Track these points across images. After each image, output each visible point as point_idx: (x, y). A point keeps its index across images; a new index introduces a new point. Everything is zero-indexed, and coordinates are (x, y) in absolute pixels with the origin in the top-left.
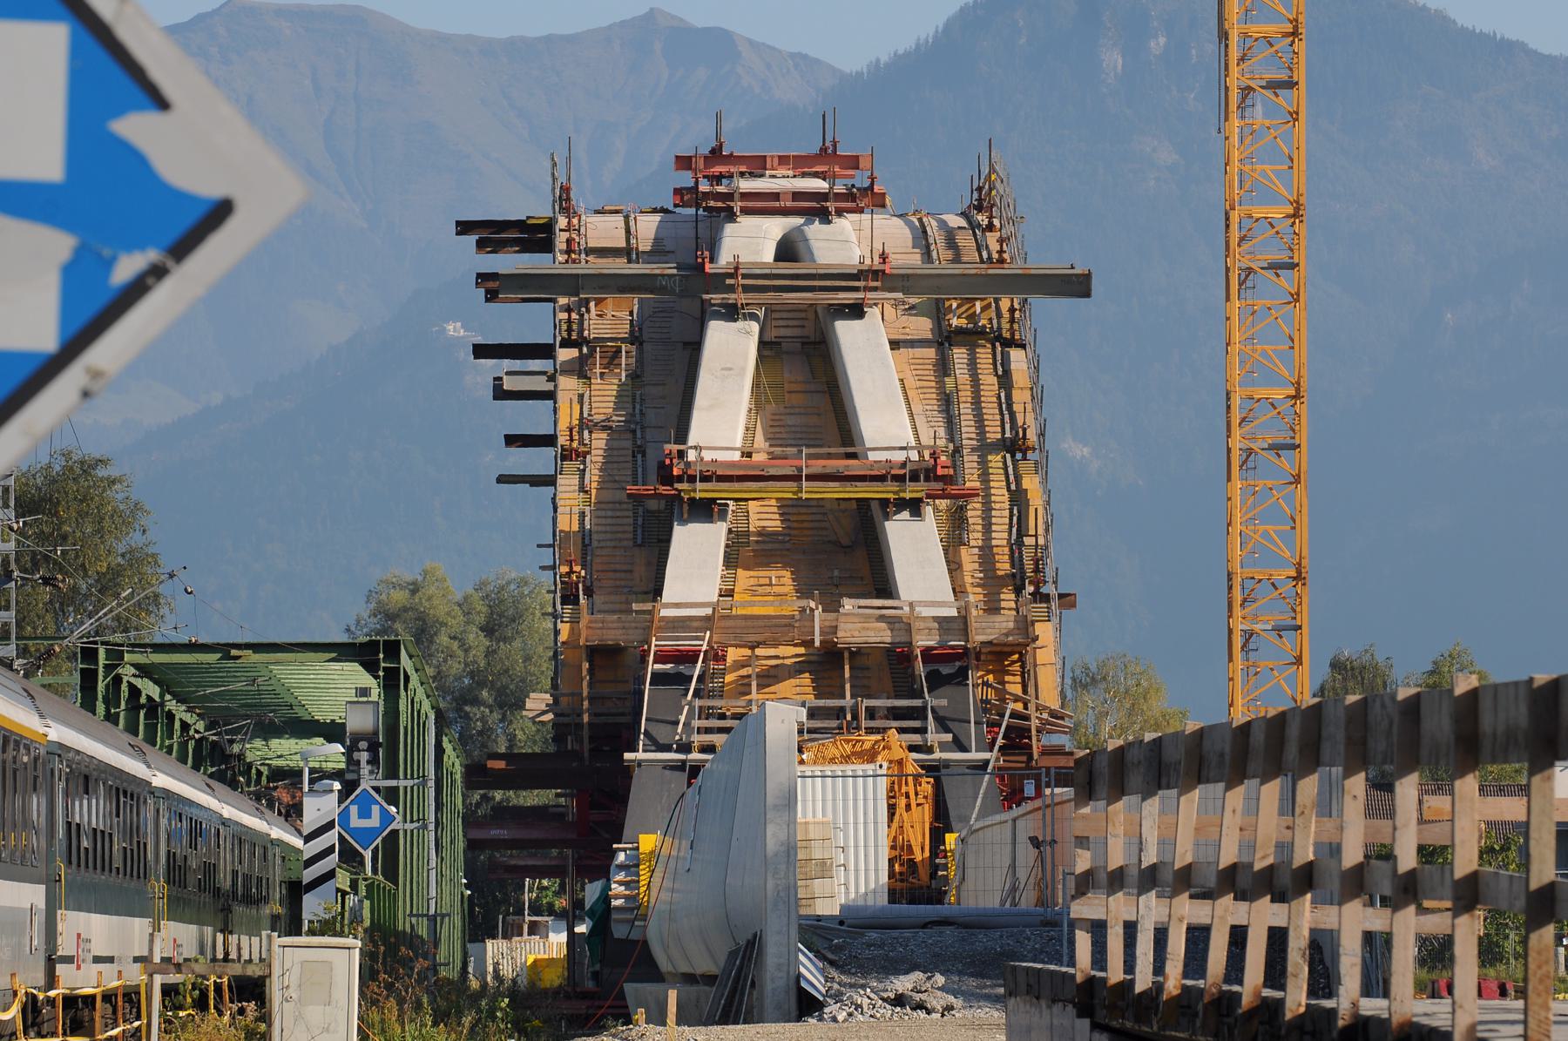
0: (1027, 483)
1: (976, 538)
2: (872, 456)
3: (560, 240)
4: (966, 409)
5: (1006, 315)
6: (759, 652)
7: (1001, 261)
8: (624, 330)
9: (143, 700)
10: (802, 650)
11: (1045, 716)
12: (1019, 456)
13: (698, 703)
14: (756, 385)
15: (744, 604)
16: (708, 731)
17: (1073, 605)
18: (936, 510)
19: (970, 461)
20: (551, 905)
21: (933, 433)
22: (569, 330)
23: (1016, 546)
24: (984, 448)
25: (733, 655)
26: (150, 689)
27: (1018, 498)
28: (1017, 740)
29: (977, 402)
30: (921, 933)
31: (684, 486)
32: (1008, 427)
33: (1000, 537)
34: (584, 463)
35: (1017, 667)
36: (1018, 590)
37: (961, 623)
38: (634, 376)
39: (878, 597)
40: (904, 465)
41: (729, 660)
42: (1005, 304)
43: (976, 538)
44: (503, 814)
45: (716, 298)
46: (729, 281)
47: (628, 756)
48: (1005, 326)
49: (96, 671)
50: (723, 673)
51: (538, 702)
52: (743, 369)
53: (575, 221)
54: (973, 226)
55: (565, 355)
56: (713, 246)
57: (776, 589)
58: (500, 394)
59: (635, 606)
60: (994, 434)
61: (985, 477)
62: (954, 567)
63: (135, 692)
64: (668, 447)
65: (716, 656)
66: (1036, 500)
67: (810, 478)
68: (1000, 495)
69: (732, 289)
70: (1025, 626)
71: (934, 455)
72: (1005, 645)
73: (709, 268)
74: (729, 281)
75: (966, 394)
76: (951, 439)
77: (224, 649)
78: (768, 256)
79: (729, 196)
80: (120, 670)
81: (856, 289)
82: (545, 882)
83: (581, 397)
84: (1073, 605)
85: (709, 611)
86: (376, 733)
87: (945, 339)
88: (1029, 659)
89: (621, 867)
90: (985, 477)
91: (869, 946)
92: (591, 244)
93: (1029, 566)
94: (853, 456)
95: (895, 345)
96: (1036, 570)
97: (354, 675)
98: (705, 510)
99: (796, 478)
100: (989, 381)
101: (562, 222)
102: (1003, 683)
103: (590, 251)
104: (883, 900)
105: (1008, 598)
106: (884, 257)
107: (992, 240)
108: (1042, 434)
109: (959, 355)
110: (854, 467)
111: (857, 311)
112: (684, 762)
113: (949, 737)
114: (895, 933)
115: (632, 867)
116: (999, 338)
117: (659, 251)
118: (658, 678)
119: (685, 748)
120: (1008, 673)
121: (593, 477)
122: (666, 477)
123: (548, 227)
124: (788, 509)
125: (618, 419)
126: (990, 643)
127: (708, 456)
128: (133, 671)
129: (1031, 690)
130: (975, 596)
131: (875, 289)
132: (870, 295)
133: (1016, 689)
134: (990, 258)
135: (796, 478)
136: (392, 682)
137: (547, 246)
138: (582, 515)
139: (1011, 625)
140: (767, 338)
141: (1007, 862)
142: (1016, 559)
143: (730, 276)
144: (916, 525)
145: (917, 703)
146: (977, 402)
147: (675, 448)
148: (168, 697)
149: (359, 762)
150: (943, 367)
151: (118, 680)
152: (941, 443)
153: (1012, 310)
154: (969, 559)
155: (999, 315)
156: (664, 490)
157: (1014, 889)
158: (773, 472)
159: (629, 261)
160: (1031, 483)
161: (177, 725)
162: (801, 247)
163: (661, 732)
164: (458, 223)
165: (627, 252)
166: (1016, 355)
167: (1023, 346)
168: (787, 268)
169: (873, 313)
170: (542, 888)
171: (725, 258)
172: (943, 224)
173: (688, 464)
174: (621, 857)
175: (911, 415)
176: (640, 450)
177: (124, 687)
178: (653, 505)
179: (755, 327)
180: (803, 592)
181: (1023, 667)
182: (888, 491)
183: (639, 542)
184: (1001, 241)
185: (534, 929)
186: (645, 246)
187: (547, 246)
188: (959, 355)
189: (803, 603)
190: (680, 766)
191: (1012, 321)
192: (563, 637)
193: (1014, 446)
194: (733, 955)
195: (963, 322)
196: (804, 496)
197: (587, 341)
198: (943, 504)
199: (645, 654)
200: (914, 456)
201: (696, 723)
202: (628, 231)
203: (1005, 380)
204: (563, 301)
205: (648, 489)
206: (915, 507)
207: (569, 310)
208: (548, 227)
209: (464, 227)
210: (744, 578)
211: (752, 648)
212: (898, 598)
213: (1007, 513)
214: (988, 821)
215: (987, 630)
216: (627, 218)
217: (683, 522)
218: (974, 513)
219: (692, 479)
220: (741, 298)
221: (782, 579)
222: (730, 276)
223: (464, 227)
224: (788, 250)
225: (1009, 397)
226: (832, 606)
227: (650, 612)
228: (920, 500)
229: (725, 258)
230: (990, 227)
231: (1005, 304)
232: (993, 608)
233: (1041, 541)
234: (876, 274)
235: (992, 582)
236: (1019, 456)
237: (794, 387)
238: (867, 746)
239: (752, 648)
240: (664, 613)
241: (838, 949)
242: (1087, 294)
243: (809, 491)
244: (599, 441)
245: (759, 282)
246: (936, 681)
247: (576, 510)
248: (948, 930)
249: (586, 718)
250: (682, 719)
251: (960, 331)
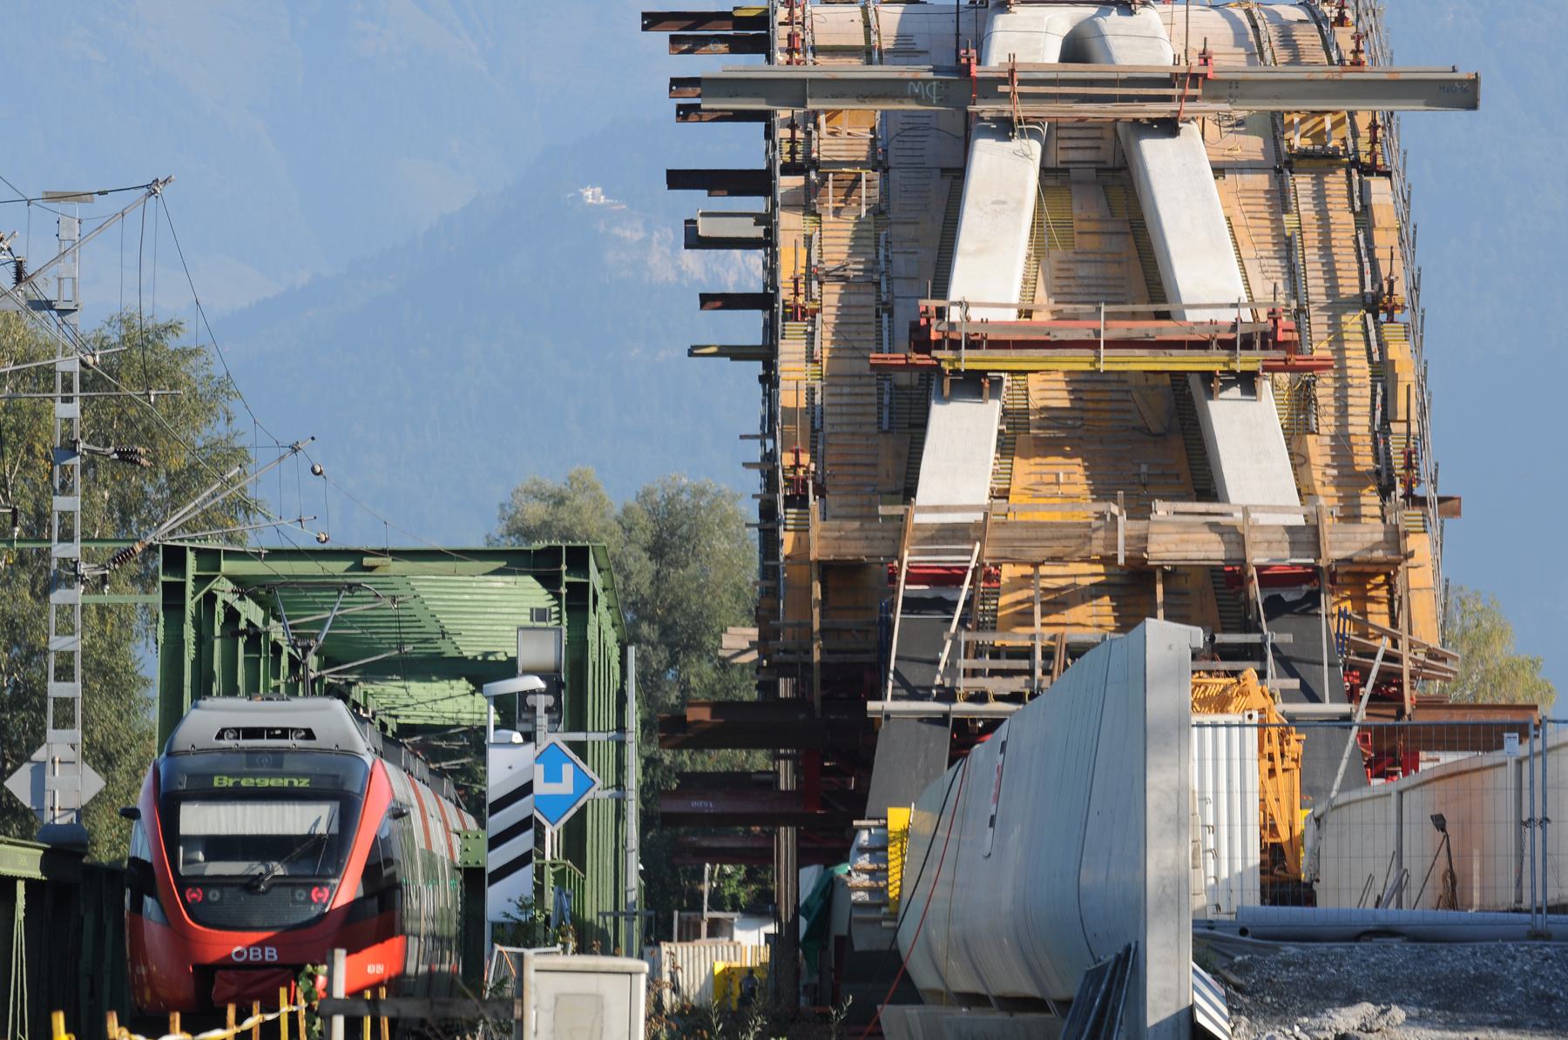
0: (1393, 352)
1: (1327, 422)
2: (1192, 316)
3: (780, 35)
4: (1312, 255)
5: (1365, 134)
6: (1043, 570)
7: (1357, 63)
8: (862, 152)
9: (243, 625)
10: (1100, 568)
11: (1421, 657)
12: (1383, 316)
13: (964, 637)
14: (1038, 224)
15: (1025, 508)
16: (975, 673)
17: (1456, 512)
18: (1275, 386)
19: (1319, 323)
20: (734, 897)
21: (1268, 285)
22: (793, 152)
23: (1381, 432)
24: (1337, 306)
25: (1008, 572)
26: (251, 612)
27: (1383, 372)
28: (1387, 693)
29: (1326, 247)
30: (1357, 947)
31: (945, 354)
32: (1368, 278)
33: (1360, 424)
34: (813, 323)
35: (1382, 593)
36: (1385, 492)
37: (1307, 536)
38: (877, 212)
39: (1199, 500)
40: (1234, 327)
41: (1004, 579)
42: (1363, 121)
43: (1327, 422)
44: (694, 783)
45: (986, 109)
46: (1002, 88)
47: (872, 705)
48: (1364, 146)
49: (183, 585)
50: (997, 594)
51: (739, 639)
52: (1021, 203)
53: (798, 11)
54: (1319, 20)
55: (787, 183)
56: (981, 43)
57: (1064, 489)
58: (695, 240)
59: (882, 510)
60: (1349, 286)
61: (1338, 341)
62: (1299, 461)
63: (232, 615)
64: (923, 303)
65: (988, 575)
66: (1406, 375)
67: (1110, 344)
68: (1359, 369)
69: (1005, 96)
70: (1395, 538)
71: (1273, 314)
72: (1369, 563)
73: (976, 71)
74: (1002, 88)
75: (1312, 237)
76: (1294, 294)
77: (355, 555)
78: (1050, 53)
80: (213, 585)
81: (1168, 99)
82: (728, 869)
83: (808, 239)
84: (1456, 512)
85: (979, 517)
86: (558, 671)
87: (1283, 164)
88: (1399, 581)
89: (862, 850)
90: (1338, 341)
91: (1287, 964)
92: (820, 42)
93: (1398, 461)
94: (1165, 316)
95: (1219, 171)
96: (1409, 466)
97: (529, 593)
98: (973, 385)
99: (1094, 345)
100: (1342, 218)
101: (782, 14)
102: (1364, 613)
103: (816, 50)
104: (1253, 899)
105: (1370, 501)
106: (1205, 58)
107: (1344, 39)
108: (1415, 288)
109: (1302, 184)
110: (1168, 330)
111: (1168, 127)
112: (946, 715)
113: (1295, 684)
114: (1322, 947)
115: (879, 850)
116: (1356, 163)
117: (905, 49)
118: (912, 604)
119: (948, 695)
120: (1373, 600)
121: (825, 338)
122: (921, 340)
123: (763, 20)
124: (1079, 383)
125: (856, 268)
126: (1348, 561)
127: (976, 315)
128: (230, 586)
129: (1403, 623)
130: (1328, 498)
131: (1194, 98)
132: (1187, 106)
133: (1383, 621)
134: (1341, 61)
135: (1094, 345)
136: (577, 602)
137: (762, 45)
138: (811, 392)
139: (1379, 537)
140: (1050, 164)
141: (1392, 847)
142: (1381, 452)
143: (1004, 81)
144: (1248, 408)
145: (1254, 638)
146: (1326, 247)
147: (933, 304)
148: (273, 622)
149: (534, 709)
150: (1281, 200)
151: (210, 598)
152: (1281, 299)
153: (1373, 127)
154: (1318, 448)
155: (1355, 134)
156: (916, 358)
157: (1399, 887)
158: (1061, 336)
159: (869, 62)
160: (1399, 352)
161: (285, 661)
162: (1095, 45)
163: (915, 675)
164: (645, 15)
165: (867, 53)
166: (1378, 185)
167: (1388, 175)
168: (1076, 70)
169: (1190, 131)
170: (722, 875)
171: (996, 59)
172: (1275, 17)
173: (952, 326)
174: (864, 837)
175: (1241, 261)
176: (886, 308)
177: (219, 607)
178: (903, 378)
179: (1035, 147)
180: (1102, 491)
181: (1391, 591)
182: (1213, 361)
183: (885, 427)
184: (1357, 38)
185: (716, 929)
186: (888, 44)
187: (762, 45)
188: (1302, 184)
189: (1101, 507)
190: (943, 720)
191: (1374, 141)
192: (786, 549)
193: (1377, 304)
194: (1094, 976)
195: (1307, 143)
196: (1103, 367)
197: (815, 164)
198: (1284, 378)
199: (893, 578)
200: (1247, 316)
201: (963, 663)
202: (867, 26)
203: (1364, 217)
204: (784, 113)
205: (898, 358)
206: (1247, 382)
207: (792, 126)
208: (763, 20)
209: (652, 21)
210: (1025, 470)
211: (1036, 565)
212: (1226, 500)
213: (1368, 391)
214: (1355, 795)
215: (1341, 544)
216: (865, 9)
217: (945, 400)
218: (1324, 391)
219: (955, 345)
220: (1019, 110)
221: (1072, 474)
222: (1004, 81)
223: (652, 21)
224: (1076, 48)
225: (1369, 240)
226: (1140, 511)
227: (901, 518)
228: (1254, 374)
229: (996, 59)
230: (1341, 20)
231: (1363, 121)
232: (1351, 515)
233: (1414, 428)
234: (1195, 79)
235: (1349, 479)
236: (1383, 316)
237: (1086, 226)
238: (1212, 691)
239: (1036, 565)
240: (919, 518)
241: (1242, 969)
242: (1473, 105)
243: (1111, 361)
244: (831, 296)
245: (1041, 86)
246: (1276, 608)
247: (803, 385)
248: (1396, 944)
249: (817, 656)
250: (944, 657)
251: (1304, 155)
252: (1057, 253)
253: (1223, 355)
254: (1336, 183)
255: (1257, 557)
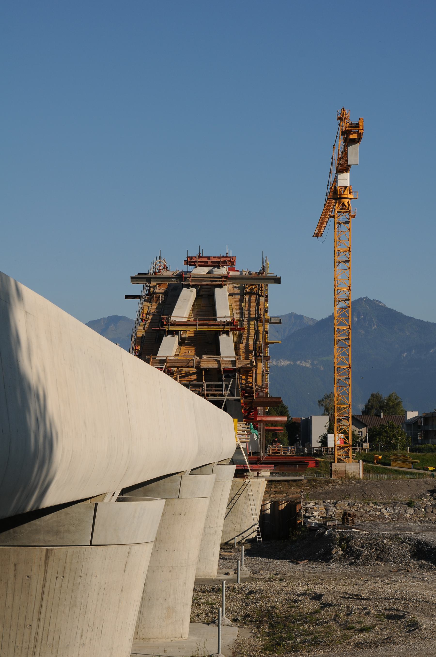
24: (250, 319)
27: (257, 332)
32: (257, 314)
37: (234, 363)
60: (253, 316)
79: (196, 262)
83: (149, 307)
87: (243, 294)
100: (253, 303)
111: (220, 286)
150: (241, 301)
169: (225, 288)
193: (258, 319)
203: (258, 304)
206: (227, 333)
217: (166, 336)
225: (258, 308)
252: (196, 310)
253: (222, 327)
254: (253, 297)
255: (223, 366)
